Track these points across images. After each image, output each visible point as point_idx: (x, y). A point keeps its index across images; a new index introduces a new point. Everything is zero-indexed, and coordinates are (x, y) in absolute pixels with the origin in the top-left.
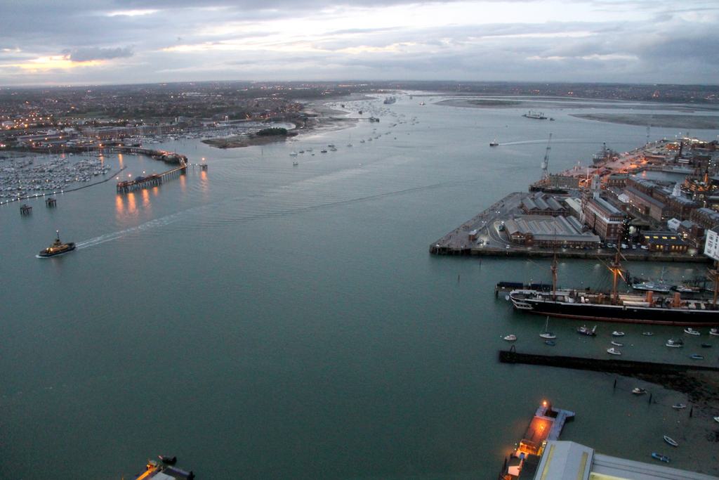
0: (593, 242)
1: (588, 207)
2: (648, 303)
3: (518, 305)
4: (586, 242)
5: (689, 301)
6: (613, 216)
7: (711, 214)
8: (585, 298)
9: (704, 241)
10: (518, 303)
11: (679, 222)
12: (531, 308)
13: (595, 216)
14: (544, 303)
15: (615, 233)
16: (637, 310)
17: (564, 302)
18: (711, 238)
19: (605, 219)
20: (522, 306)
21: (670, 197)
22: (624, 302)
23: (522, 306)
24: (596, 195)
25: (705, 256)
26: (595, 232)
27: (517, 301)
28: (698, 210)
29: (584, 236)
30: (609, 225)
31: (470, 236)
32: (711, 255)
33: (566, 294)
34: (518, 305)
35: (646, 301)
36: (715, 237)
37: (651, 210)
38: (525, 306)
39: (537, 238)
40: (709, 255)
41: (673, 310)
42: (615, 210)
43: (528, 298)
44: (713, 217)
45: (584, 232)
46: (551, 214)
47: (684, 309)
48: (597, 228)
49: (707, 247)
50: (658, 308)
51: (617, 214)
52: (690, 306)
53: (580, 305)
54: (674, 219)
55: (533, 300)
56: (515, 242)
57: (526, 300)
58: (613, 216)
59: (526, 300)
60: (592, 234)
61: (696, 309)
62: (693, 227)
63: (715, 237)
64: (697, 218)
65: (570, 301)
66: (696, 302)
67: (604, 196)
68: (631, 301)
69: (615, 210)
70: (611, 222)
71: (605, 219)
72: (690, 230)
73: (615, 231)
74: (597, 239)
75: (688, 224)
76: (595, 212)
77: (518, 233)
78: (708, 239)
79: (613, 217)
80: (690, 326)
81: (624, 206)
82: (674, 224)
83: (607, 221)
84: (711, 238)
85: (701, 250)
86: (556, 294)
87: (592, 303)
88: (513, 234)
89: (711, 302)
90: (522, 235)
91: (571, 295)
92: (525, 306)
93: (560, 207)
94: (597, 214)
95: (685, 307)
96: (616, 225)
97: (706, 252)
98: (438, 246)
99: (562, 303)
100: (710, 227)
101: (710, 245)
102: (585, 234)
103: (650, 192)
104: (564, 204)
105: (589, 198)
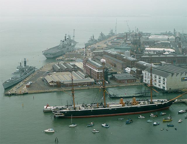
0: (91, 82)
3: (56, 115)
5: (140, 102)
6: (99, 68)
9: (143, 76)
11: (130, 69)
13: (91, 69)
16: (116, 108)
17: (80, 109)
20: (58, 114)
23: (58, 114)
24: (90, 59)
25: (144, 83)
26: (91, 78)
27: (56, 112)
28: (137, 62)
29: (86, 80)
31: (27, 86)
32: (147, 82)
33: (80, 106)
34: (56, 115)
36: (147, 74)
38: (60, 114)
42: (100, 65)
43: (61, 110)
44: (145, 65)
45: (85, 78)
46: (68, 71)
47: (139, 105)
48: (92, 75)
50: (126, 106)
51: (101, 67)
52: (141, 103)
56: (51, 86)
57: (60, 111)
58: (99, 68)
59: (60, 111)
60: (90, 79)
62: (137, 70)
63: (147, 74)
64: (138, 66)
65: (83, 109)
66: (143, 101)
68: (114, 105)
69: (100, 65)
71: (95, 70)
72: (136, 72)
73: (101, 75)
74: (92, 80)
75: (134, 69)
76: (90, 67)
77: (52, 82)
79: (99, 69)
81: (103, 63)
82: (128, 70)
83: (97, 71)
84: (146, 74)
85: (142, 80)
86: (75, 107)
87: (94, 108)
88: (50, 83)
89: (150, 101)
90: (55, 82)
91: (83, 106)
92: (60, 114)
94: (91, 68)
95: (139, 104)
96: (101, 72)
98: (10, 93)
102: (87, 79)
103: (115, 56)
104: (74, 66)
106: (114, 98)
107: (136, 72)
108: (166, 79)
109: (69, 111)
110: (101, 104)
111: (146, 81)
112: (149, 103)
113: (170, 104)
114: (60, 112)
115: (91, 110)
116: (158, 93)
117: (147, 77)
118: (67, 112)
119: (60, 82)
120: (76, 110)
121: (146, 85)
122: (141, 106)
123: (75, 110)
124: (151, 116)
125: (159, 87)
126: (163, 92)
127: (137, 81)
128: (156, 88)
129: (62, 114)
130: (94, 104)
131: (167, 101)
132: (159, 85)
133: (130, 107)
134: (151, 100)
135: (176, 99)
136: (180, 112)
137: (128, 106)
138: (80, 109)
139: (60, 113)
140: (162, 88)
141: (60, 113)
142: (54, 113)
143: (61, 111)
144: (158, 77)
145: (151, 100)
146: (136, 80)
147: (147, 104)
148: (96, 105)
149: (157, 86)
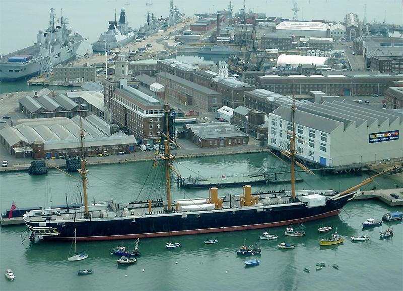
0: (127, 145)
1: (115, 99)
2: (213, 205)
3: (37, 232)
4: (118, 146)
5: (262, 196)
6: (151, 107)
7: (268, 96)
8: (130, 209)
9: (266, 130)
10: (35, 228)
11: (231, 110)
12: (56, 233)
14: (74, 223)
15: (155, 130)
17: (101, 217)
18: (274, 124)
19: (139, 112)
20: (42, 232)
21: (216, 80)
22: (183, 207)
23: (42, 232)
24: (124, 83)
25: (269, 147)
26: (128, 133)
28: (252, 92)
30: (146, 119)
32: (276, 146)
34: (37, 232)
35: (211, 202)
36: (278, 123)
37: (195, 98)
38: (47, 232)
39: (47, 148)
42: (152, 100)
43: (49, 219)
44: (271, 99)
45: (112, 132)
47: (259, 207)
49: (270, 135)
50: (226, 208)
51: (155, 103)
52: (265, 201)
53: (125, 218)
54: (225, 107)
55: (59, 220)
56: (19, 156)
60: (125, 136)
62: (250, 114)
63: (278, 123)
65: (111, 216)
67: (133, 82)
69: (152, 100)
70: (148, 116)
71: (139, 112)
72: (247, 117)
73: (155, 127)
74: (132, 140)
75: (243, 110)
76: (125, 105)
77: (21, 144)
78: (270, 127)
80: (267, 229)
81: (159, 95)
82: (226, 112)
83: (145, 115)
84: (274, 124)
88: (15, 146)
90: (28, 145)
92: (47, 232)
93: (75, 104)
94: (128, 107)
95: (260, 204)
96: (155, 118)
97: (270, 143)
99: (99, 220)
100: (271, 111)
101: (274, 133)
102: (115, 136)
103: (191, 76)
104: (79, 100)
105: (114, 88)
106: (191, 187)
107: (247, 117)
108: (328, 138)
109: (72, 221)
110: (159, 204)
111: (274, 141)
112: (287, 199)
113: (343, 202)
114: (48, 225)
115: (131, 220)
116: (307, 173)
117: (278, 134)
118: (66, 223)
119: (42, 145)
120: (93, 220)
121: (276, 152)
122: (267, 207)
123: (89, 220)
124: (286, 234)
125: (310, 158)
126: (322, 170)
127: (250, 143)
128: (301, 161)
129: (52, 231)
130: (141, 202)
131: (332, 195)
132: (311, 154)
133: (237, 209)
134: (293, 192)
136: (366, 223)
137: (231, 208)
138: (101, 217)
139: (47, 228)
140: (317, 160)
141: (47, 228)
142: (31, 227)
143: (51, 222)
144: (306, 131)
145: (293, 192)
146: (247, 139)
147: (282, 202)
148: (144, 205)
149: (305, 155)
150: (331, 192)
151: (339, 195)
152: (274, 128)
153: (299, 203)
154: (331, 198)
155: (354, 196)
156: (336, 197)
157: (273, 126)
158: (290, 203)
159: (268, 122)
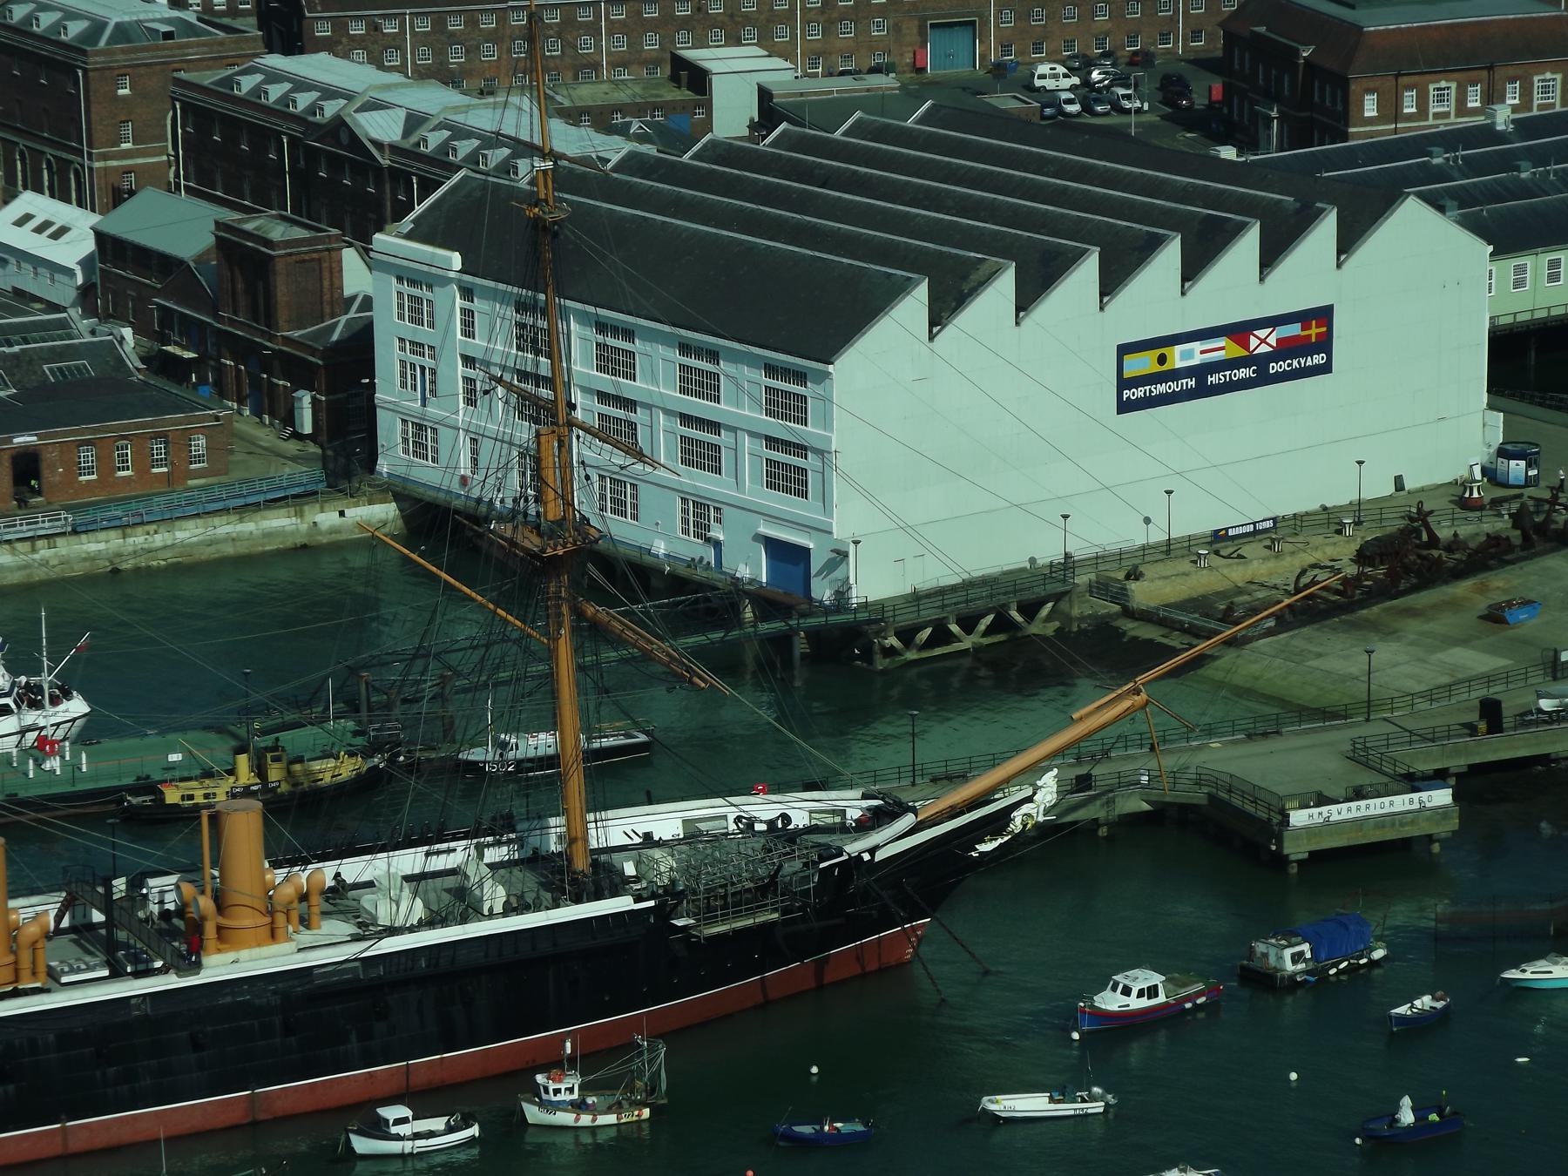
5: (353, 869)
25: (399, 492)
40: (426, 474)
41: (218, 967)
61: (433, 920)
62: (229, 245)
101: (427, 382)
131: (866, 825)
135: (1034, 771)
136: (1110, 1001)
140: (752, 567)
150: (853, 805)
151: (908, 820)
152: (417, 347)
153: (623, 904)
154: (853, 848)
155: (1016, 825)
156: (890, 842)
157: (424, 334)
158: (556, 905)
159: (367, 303)
